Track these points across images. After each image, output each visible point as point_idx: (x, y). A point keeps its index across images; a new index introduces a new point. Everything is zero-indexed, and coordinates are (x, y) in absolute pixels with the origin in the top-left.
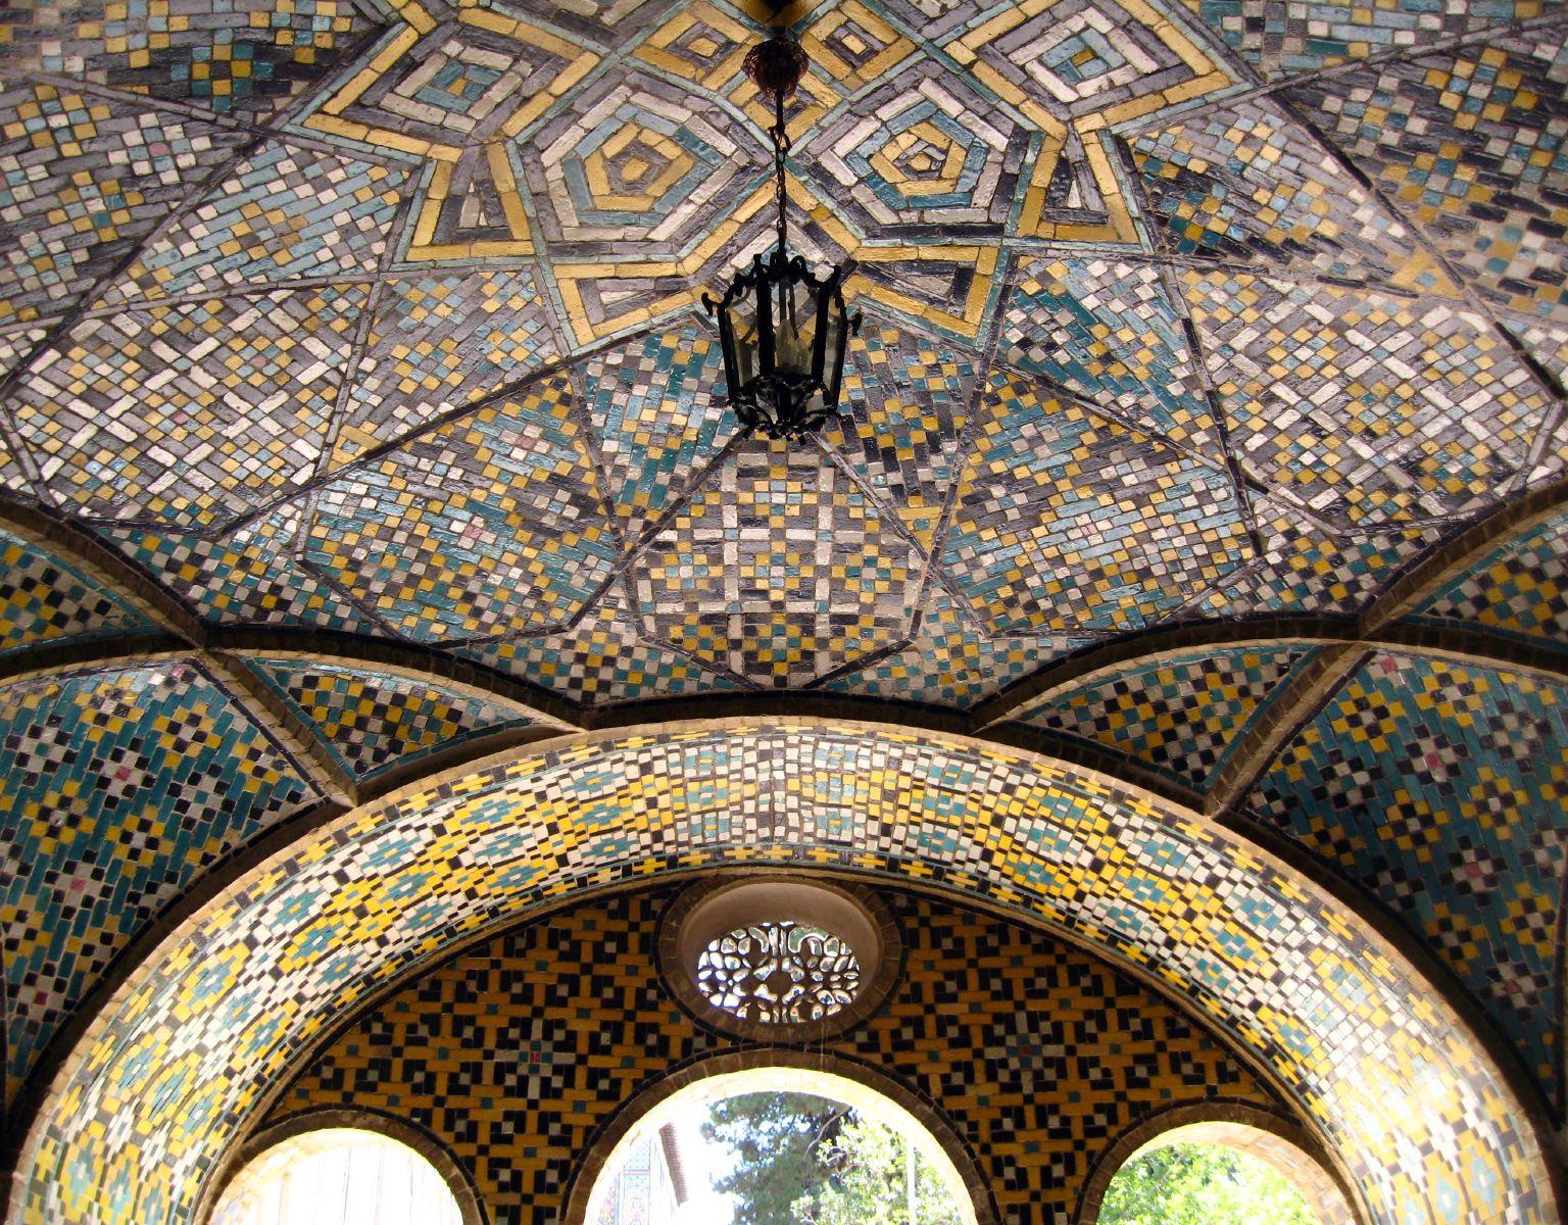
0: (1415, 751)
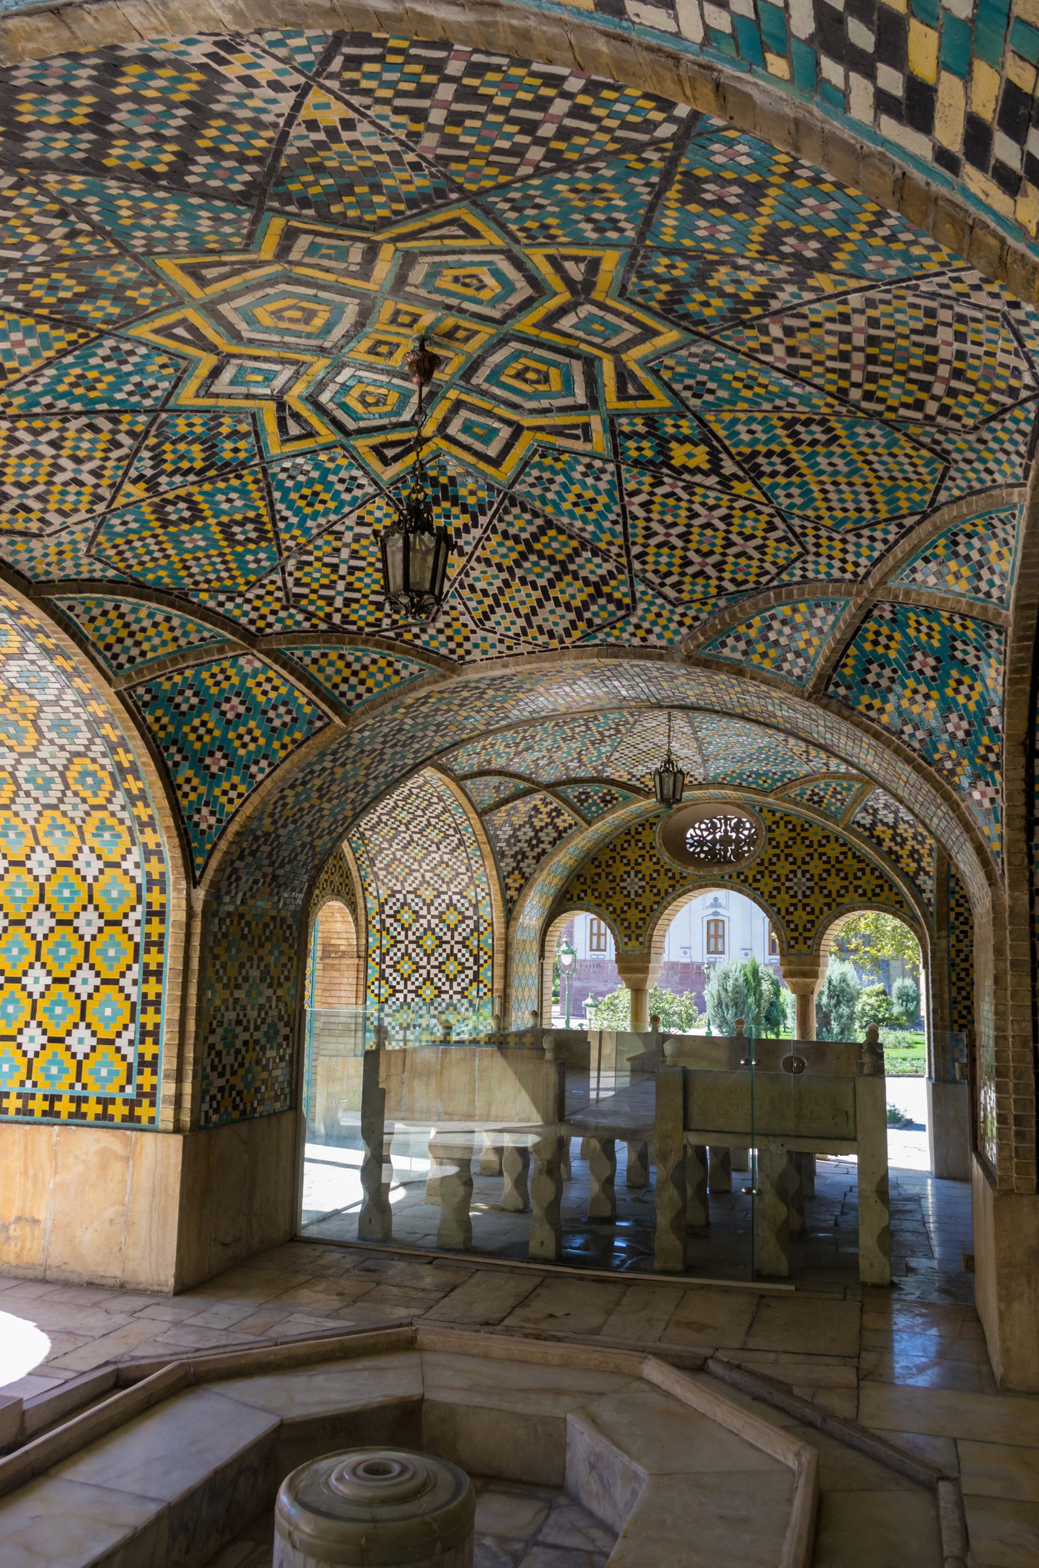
0: (228, 700)
